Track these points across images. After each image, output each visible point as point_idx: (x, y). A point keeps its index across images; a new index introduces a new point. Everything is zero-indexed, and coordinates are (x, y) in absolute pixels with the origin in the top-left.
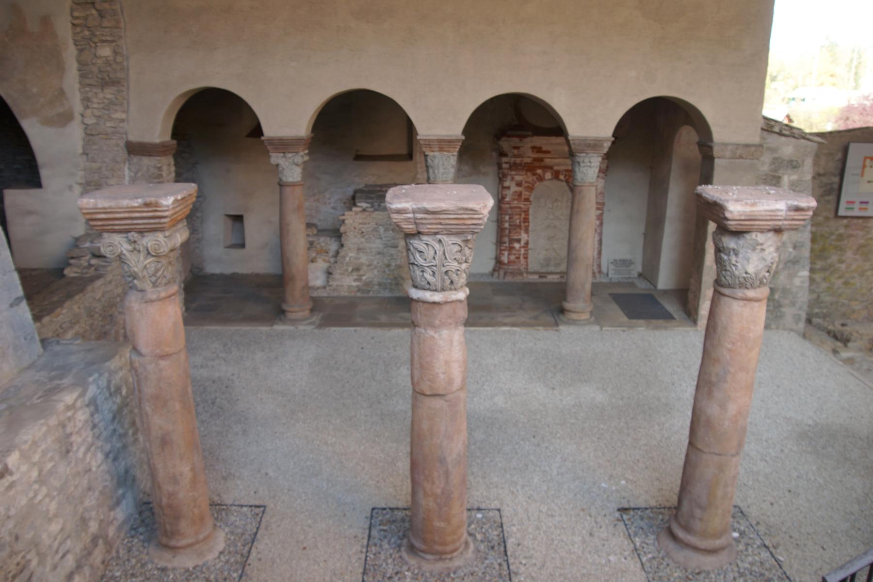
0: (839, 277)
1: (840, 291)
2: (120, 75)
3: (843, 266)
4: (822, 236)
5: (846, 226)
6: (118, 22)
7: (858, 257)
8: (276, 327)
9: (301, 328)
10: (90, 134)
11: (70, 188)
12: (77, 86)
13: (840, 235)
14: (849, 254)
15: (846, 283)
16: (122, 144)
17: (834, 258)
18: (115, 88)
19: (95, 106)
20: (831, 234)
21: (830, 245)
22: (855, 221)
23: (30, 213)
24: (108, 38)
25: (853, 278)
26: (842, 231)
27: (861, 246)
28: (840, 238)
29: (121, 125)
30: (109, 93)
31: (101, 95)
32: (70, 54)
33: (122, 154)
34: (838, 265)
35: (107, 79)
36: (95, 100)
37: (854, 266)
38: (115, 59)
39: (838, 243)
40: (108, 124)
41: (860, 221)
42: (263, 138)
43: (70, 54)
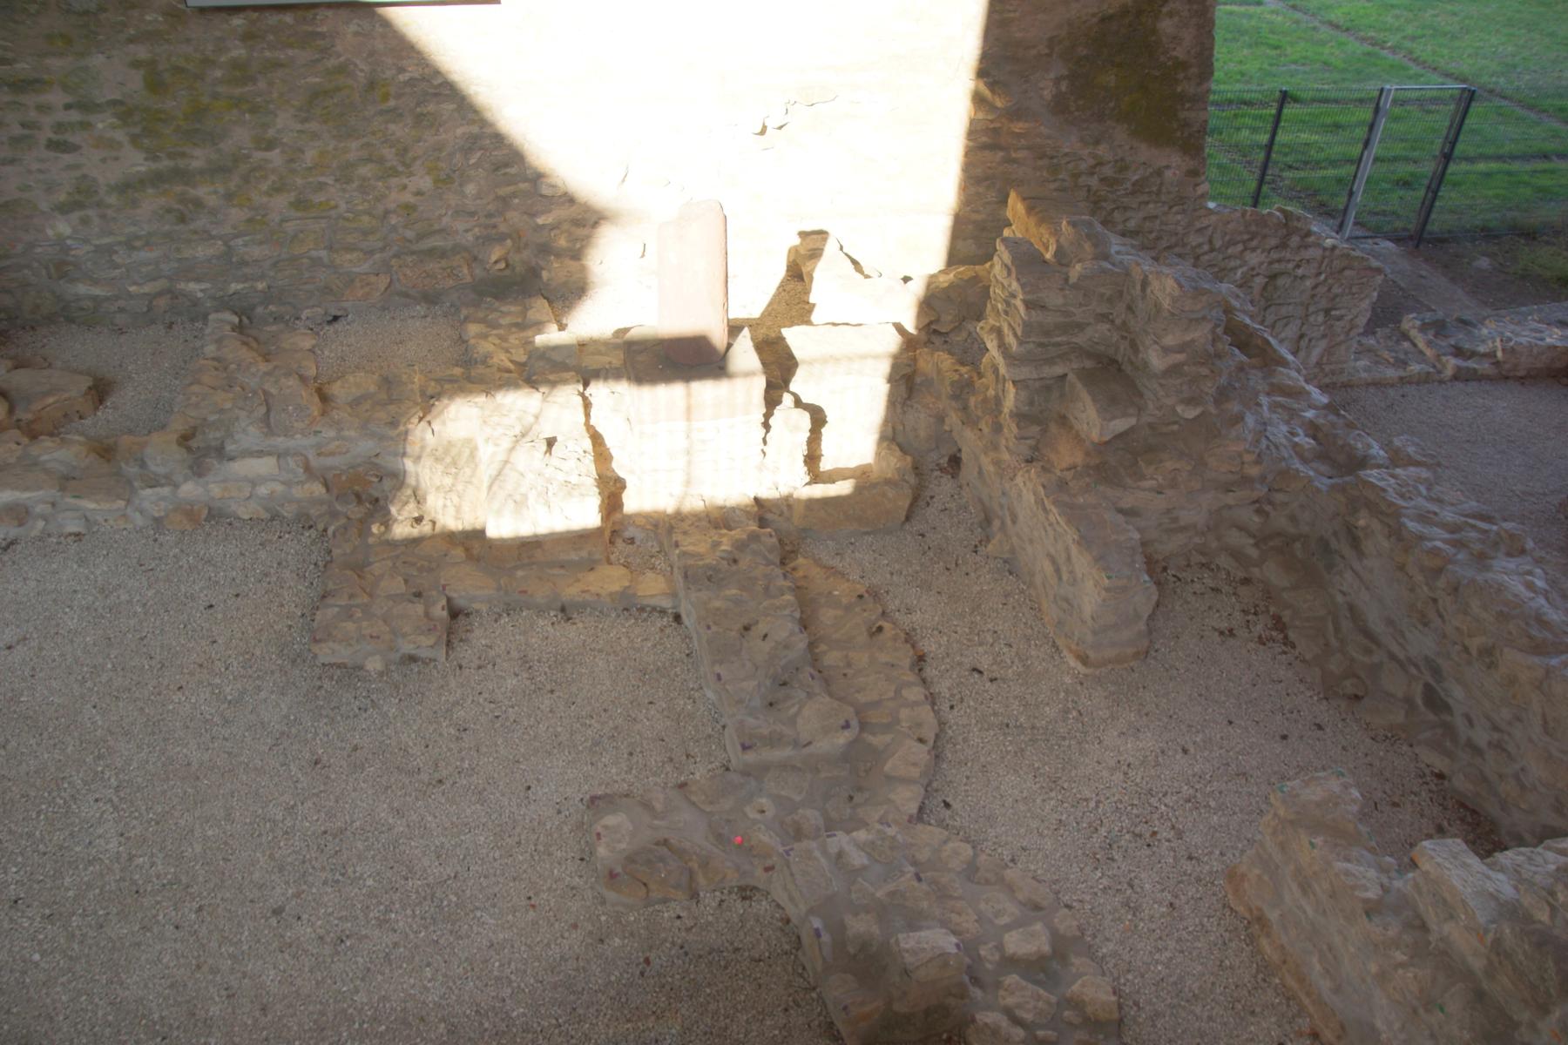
0: (277, 190)
1: (290, 227)
3: (276, 157)
4: (178, 70)
5: (248, 37)
7: (313, 126)
13: (236, 65)
14: (284, 122)
15: (300, 204)
17: (240, 136)
20: (207, 62)
21: (215, 96)
22: (273, 19)
25: (321, 187)
26: (238, 52)
27: (316, 95)
28: (241, 72)
34: (259, 155)
37: (310, 155)
39: (238, 91)
41: (288, 18)
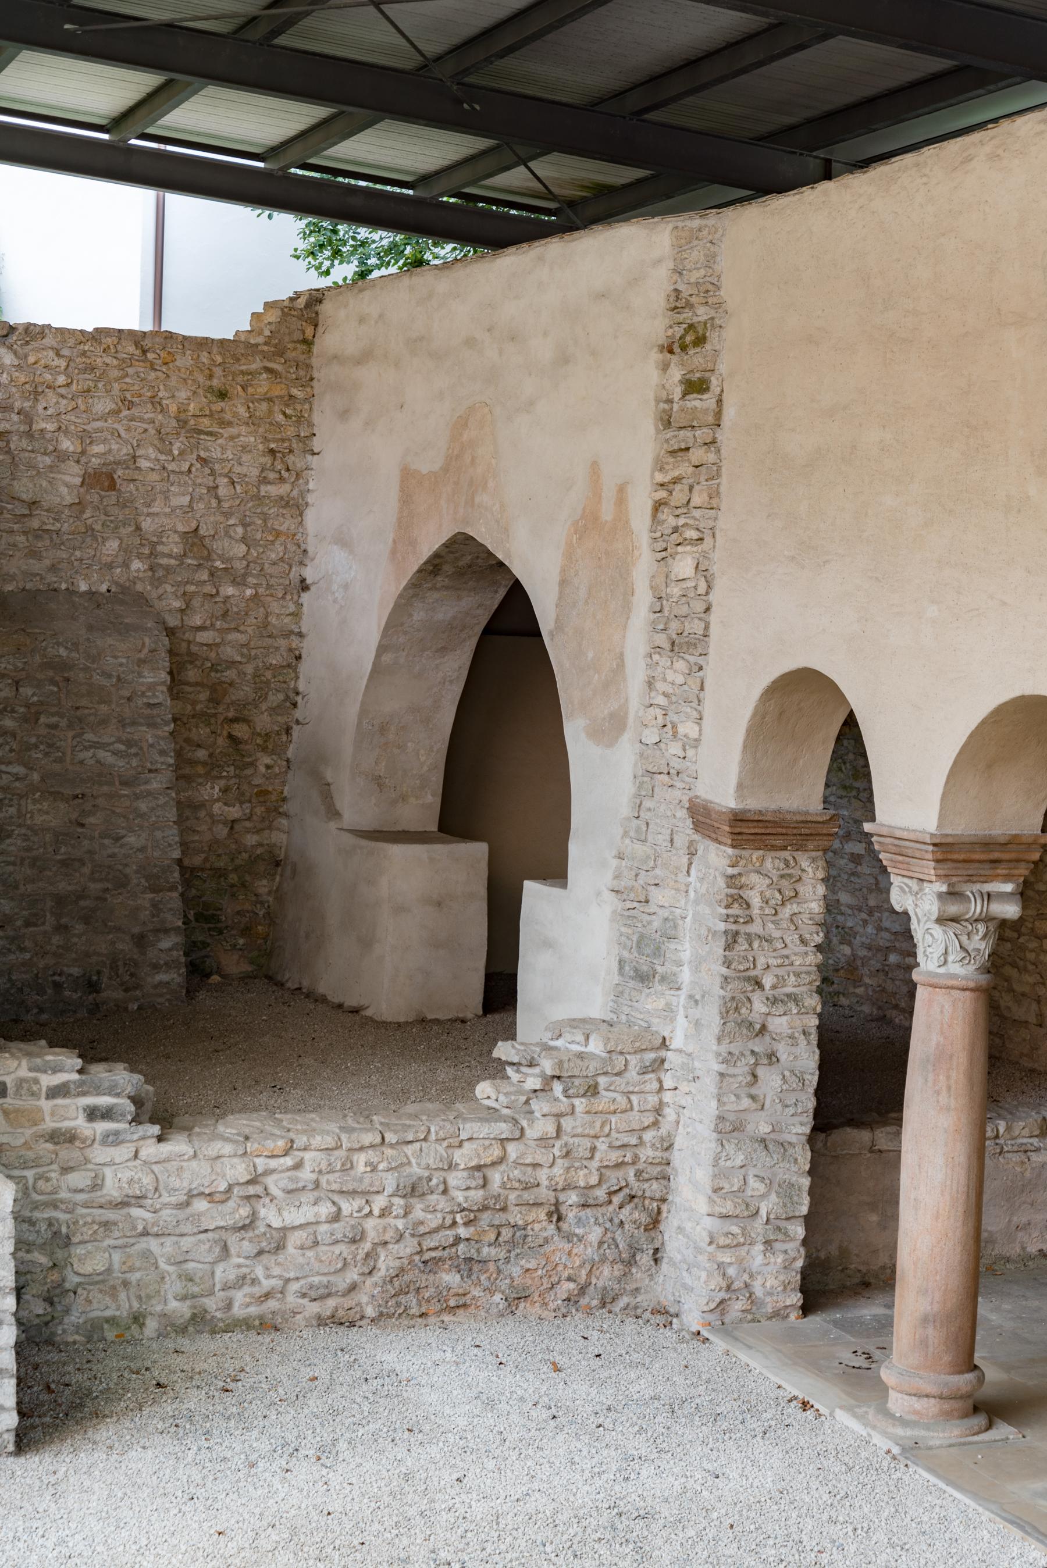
2: (698, 627)
6: (714, 494)
8: (839, 1414)
9: (877, 1439)
10: (653, 775)
11: (599, 894)
12: (643, 649)
16: (685, 799)
18: (692, 659)
19: (661, 700)
23: (548, 944)
24: (692, 534)
29: (690, 753)
30: (675, 672)
31: (670, 676)
32: (643, 568)
33: (686, 829)
35: (683, 640)
36: (660, 686)
38: (695, 588)
40: (675, 749)
42: (867, 827)
43: (643, 568)
